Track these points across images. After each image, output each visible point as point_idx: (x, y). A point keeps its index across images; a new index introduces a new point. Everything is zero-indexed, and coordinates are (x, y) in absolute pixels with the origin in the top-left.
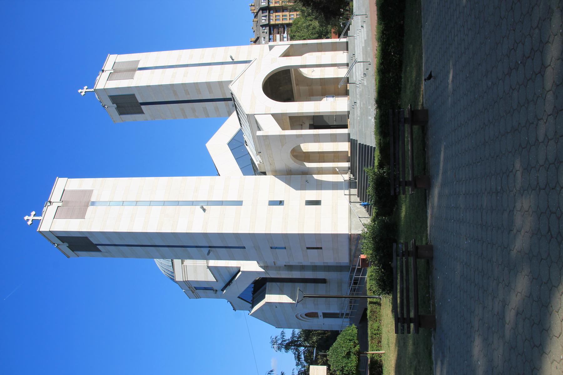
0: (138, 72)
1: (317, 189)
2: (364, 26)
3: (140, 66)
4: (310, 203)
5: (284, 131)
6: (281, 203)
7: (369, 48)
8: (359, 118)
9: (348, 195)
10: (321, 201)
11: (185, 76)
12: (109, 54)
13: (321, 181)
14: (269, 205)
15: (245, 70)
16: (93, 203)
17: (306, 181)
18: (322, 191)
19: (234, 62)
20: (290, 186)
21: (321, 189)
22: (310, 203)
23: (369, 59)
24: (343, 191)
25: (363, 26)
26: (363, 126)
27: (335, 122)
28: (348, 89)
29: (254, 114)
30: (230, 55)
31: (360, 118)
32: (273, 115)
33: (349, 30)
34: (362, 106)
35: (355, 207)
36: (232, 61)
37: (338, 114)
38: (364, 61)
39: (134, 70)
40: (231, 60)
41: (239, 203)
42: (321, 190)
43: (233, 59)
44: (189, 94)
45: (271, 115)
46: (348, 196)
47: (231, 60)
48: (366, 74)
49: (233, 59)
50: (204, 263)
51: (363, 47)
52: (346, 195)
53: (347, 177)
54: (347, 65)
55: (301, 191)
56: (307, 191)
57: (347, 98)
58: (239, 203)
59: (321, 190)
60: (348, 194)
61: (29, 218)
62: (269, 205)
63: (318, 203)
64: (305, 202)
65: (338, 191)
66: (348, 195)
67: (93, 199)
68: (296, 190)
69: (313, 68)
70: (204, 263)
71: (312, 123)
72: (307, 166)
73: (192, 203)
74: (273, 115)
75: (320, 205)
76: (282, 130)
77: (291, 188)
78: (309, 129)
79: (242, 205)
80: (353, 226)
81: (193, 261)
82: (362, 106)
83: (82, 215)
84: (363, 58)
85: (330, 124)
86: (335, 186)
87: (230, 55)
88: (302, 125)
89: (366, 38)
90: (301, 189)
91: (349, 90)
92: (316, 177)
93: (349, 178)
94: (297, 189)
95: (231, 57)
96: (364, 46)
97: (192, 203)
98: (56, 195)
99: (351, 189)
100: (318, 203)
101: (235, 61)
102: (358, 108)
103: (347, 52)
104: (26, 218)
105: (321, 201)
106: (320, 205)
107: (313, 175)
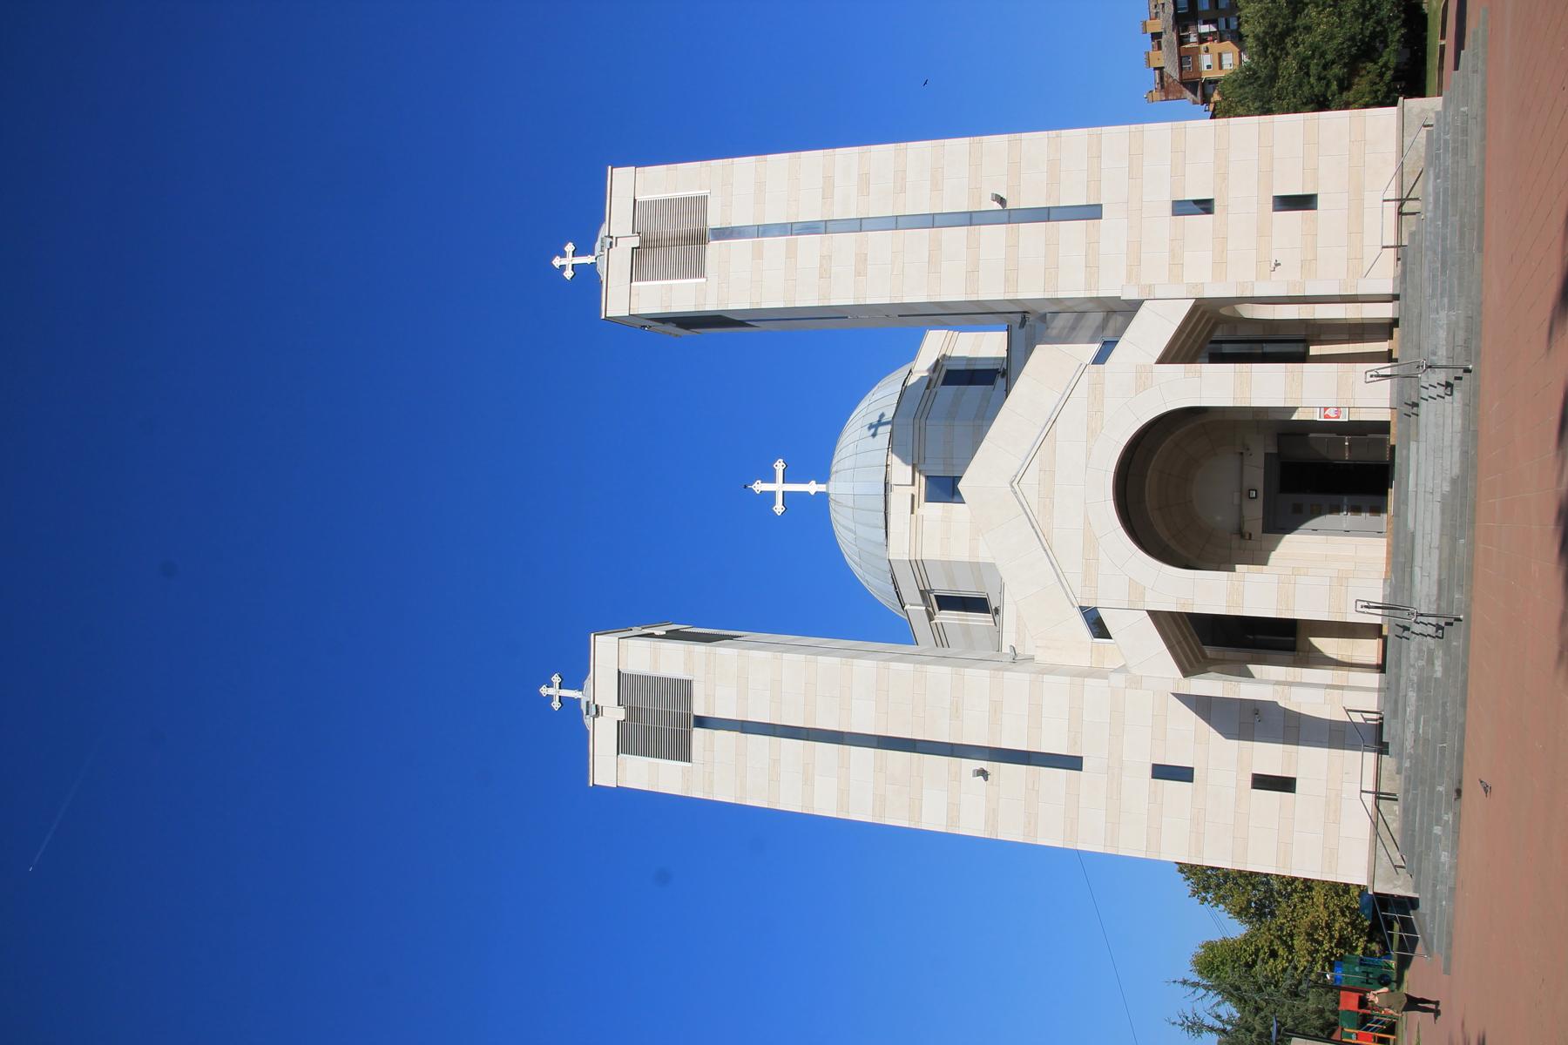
0: (714, 248)
1: (1286, 740)
3: (714, 221)
4: (1263, 782)
5: (1187, 680)
6: (1184, 774)
10: (1294, 779)
12: (610, 167)
16: (701, 722)
18: (1300, 747)
19: (1006, 214)
20: (1210, 725)
22: (1263, 782)
23: (1456, 596)
24: (1360, 753)
31: (1411, 762)
33: (1398, 327)
34: (1421, 731)
35: (1390, 814)
38: (1441, 613)
39: (699, 239)
40: (997, 206)
41: (1074, 763)
42: (1298, 745)
43: (1002, 201)
49: (1002, 201)
50: (986, 621)
51: (1443, 495)
54: (1395, 297)
55: (1241, 742)
58: (1074, 763)
61: (551, 691)
62: (1153, 777)
63: (1285, 784)
64: (1250, 778)
65: (1346, 751)
66: (1370, 792)
67: (699, 709)
68: (1227, 738)
70: (986, 621)
71: (1273, 450)
75: (1294, 792)
79: (1081, 770)
80: (1379, 871)
81: (958, 615)
82: (1421, 731)
83: (682, 752)
84: (1440, 575)
86: (1335, 735)
88: (1242, 453)
89: (1456, 471)
90: (1239, 738)
94: (1228, 735)
96: (1448, 489)
98: (602, 688)
99: (1384, 756)
100: (1285, 784)
101: (1009, 206)
102: (1409, 722)
104: (544, 691)
105: (1294, 779)
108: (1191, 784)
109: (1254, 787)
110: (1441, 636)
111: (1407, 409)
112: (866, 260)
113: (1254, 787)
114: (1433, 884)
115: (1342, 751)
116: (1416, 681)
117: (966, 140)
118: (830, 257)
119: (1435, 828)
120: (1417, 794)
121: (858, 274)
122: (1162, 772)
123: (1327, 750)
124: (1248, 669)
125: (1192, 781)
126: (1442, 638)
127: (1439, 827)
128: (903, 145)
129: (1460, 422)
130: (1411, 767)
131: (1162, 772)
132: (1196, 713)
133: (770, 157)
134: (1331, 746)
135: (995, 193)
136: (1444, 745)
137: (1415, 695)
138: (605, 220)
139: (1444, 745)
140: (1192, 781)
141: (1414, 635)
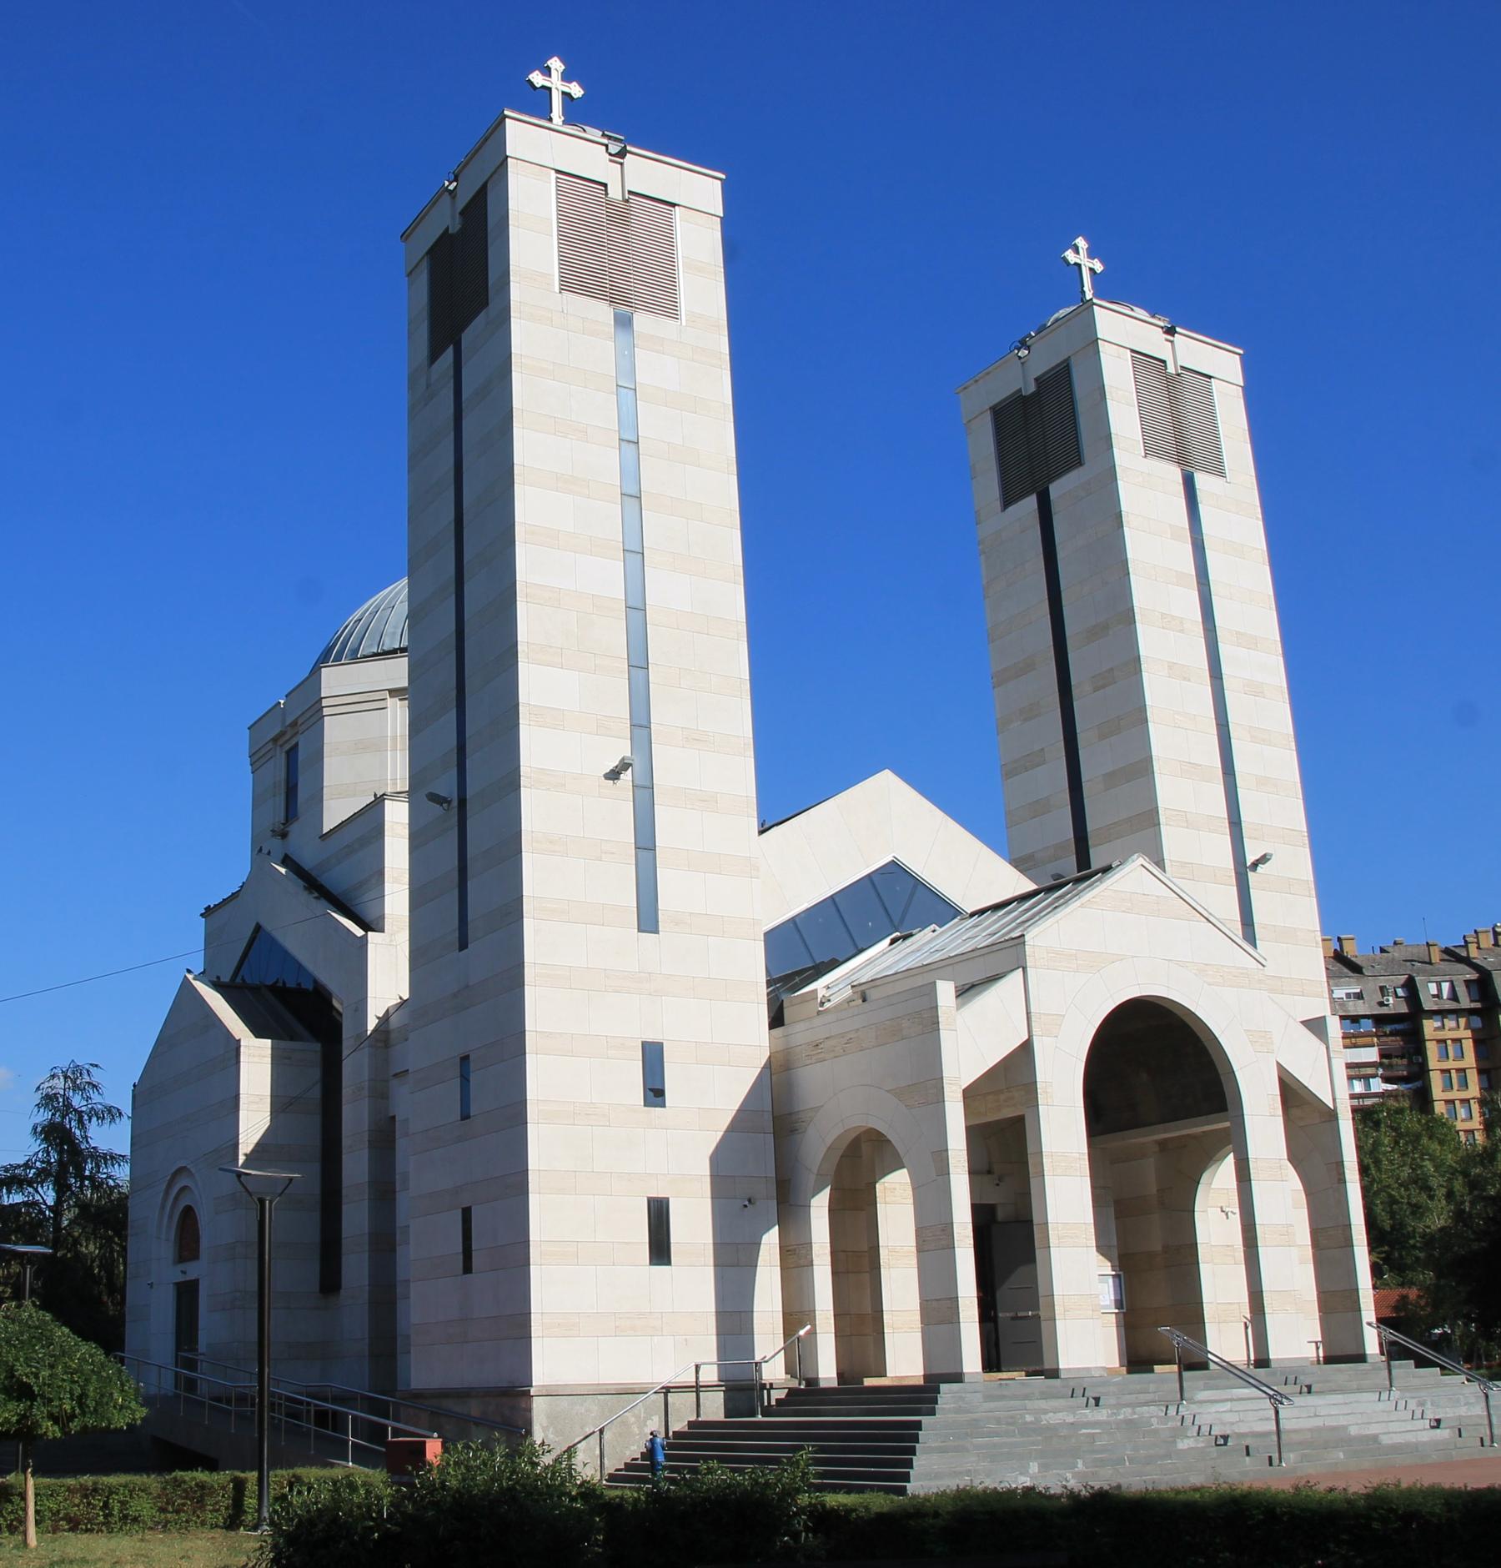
0: (1174, 473)
2: (1438, 1431)
3: (1202, 480)
6: (655, 1094)
7: (1341, 1455)
8: (1029, 1418)
9: (697, 1378)
11: (1170, 668)
13: (753, 1265)
14: (645, 1045)
15: (1212, 919)
17: (750, 1201)
18: (711, 1269)
19: (1243, 871)
20: (726, 1132)
21: (718, 1264)
24: (715, 1359)
25: (1438, 1427)
26: (996, 1439)
27: (1008, 1315)
28: (1155, 1367)
29: (1024, 969)
30: (1271, 855)
31: (1031, 1423)
32: (1026, 1049)
34: (1084, 1431)
36: (1248, 864)
37: (1044, 1325)
38: (1283, 1436)
39: (1182, 457)
40: (1250, 860)
41: (648, 920)
42: (715, 1266)
43: (1255, 865)
44: (1096, 689)
45: (1027, 1037)
46: (691, 1380)
47: (1250, 860)
48: (1225, 1444)
49: (1255, 865)
51: (1345, 1428)
52: (697, 1372)
53: (774, 1372)
54: (1262, 1362)
55: (708, 1180)
56: (709, 1201)
57: (1117, 1365)
58: (648, 920)
59: (716, 1265)
60: (700, 1379)
63: (660, 1250)
64: (661, 1195)
65: (714, 1338)
66: (697, 1378)
69: (1237, 1210)
71: (1001, 1215)
72: (815, 1202)
73: (641, 725)
74: (1026, 1049)
75: (652, 1263)
76: (963, 1088)
77: (720, 1134)
78: (973, 1206)
79: (639, 930)
82: (1084, 1431)
85: (999, 1295)
87: (1271, 855)
88: (989, 1172)
89: (1386, 1440)
90: (715, 1177)
91: (1152, 1371)
92: (771, 1239)
93: (771, 1384)
94: (718, 1159)
95: (1264, 859)
96: (1353, 1433)
97: (641, 725)
100: (660, 1250)
101: (1250, 874)
102: (1074, 1413)
103: (1318, 1360)
105: (668, 1262)
106: (652, 1263)
107: (777, 1227)
108: (642, 1104)
109: (650, 1201)
110: (1218, 1443)
111: (1291, 1379)
112: (1184, 679)
113: (650, 1201)
114: (970, 1471)
115: (714, 1331)
116: (1119, 1417)
117: (1303, 826)
118: (1182, 631)
119: (1036, 1464)
120: (1014, 1436)
121: (1171, 666)
122: (653, 1057)
123: (714, 1310)
124: (824, 1188)
125: (645, 1105)
126: (1217, 1445)
127: (1037, 1471)
128: (1293, 745)
129: (1425, 1439)
130: (1026, 1423)
131: (653, 1057)
132: (738, 1111)
133: (1267, 569)
134: (720, 1314)
135: (1273, 857)
136: (1127, 1463)
137: (1105, 1418)
138: (1153, 317)
139: (1127, 1463)
140: (645, 1105)
141: (1164, 1409)
